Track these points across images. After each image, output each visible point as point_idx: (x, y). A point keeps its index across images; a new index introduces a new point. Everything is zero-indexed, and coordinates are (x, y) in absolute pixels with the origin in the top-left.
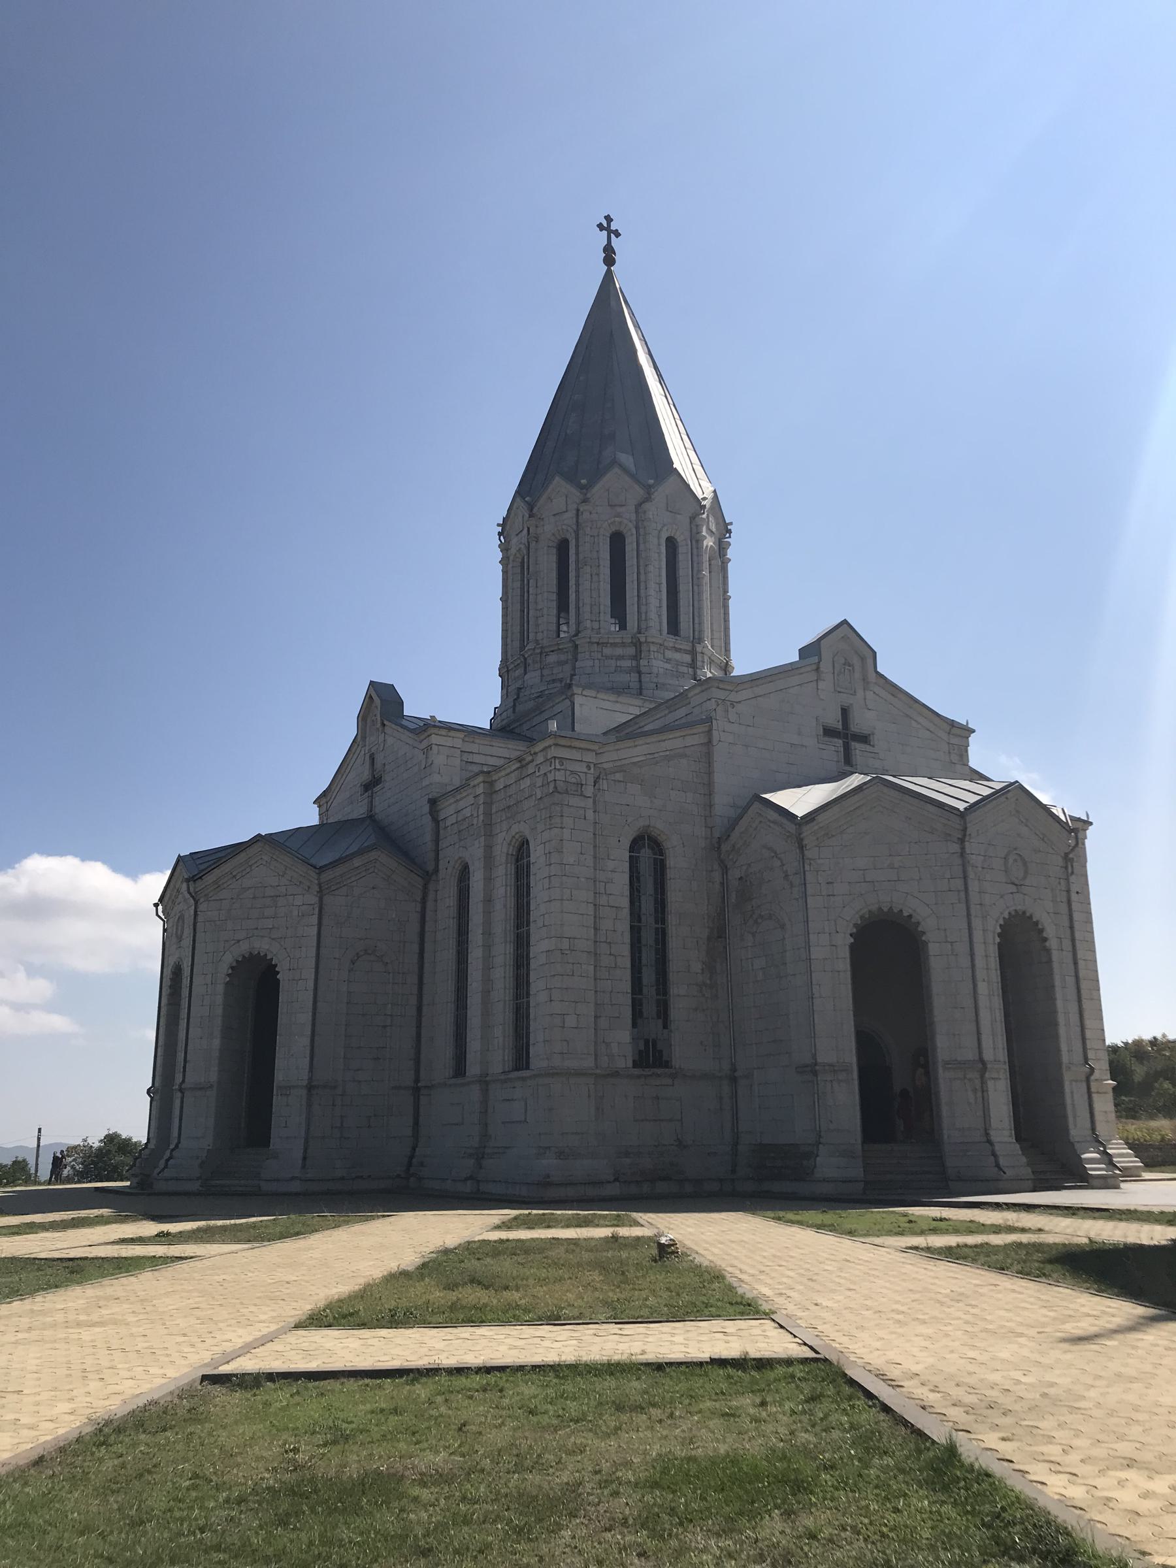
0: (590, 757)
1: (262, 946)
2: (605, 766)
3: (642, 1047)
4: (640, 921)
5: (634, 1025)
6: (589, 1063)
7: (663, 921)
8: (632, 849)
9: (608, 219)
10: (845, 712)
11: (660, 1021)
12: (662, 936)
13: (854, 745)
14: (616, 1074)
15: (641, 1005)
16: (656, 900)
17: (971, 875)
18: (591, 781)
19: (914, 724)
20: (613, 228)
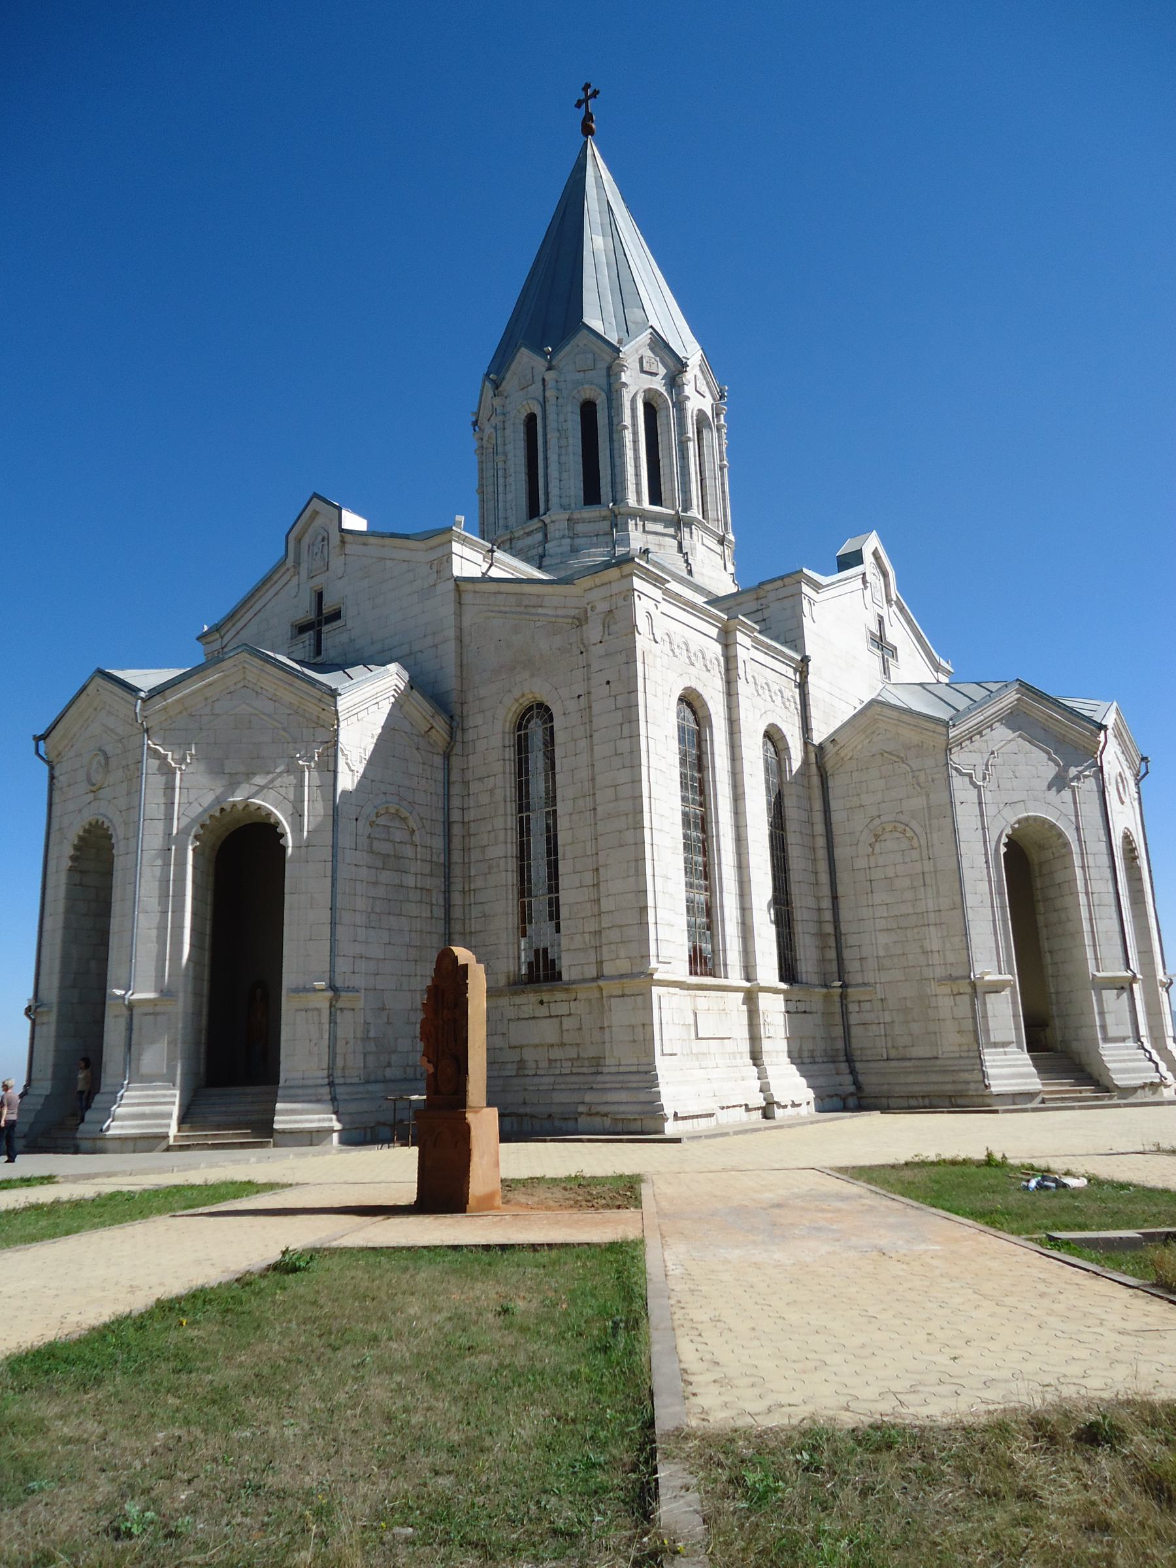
19: (389, 563)
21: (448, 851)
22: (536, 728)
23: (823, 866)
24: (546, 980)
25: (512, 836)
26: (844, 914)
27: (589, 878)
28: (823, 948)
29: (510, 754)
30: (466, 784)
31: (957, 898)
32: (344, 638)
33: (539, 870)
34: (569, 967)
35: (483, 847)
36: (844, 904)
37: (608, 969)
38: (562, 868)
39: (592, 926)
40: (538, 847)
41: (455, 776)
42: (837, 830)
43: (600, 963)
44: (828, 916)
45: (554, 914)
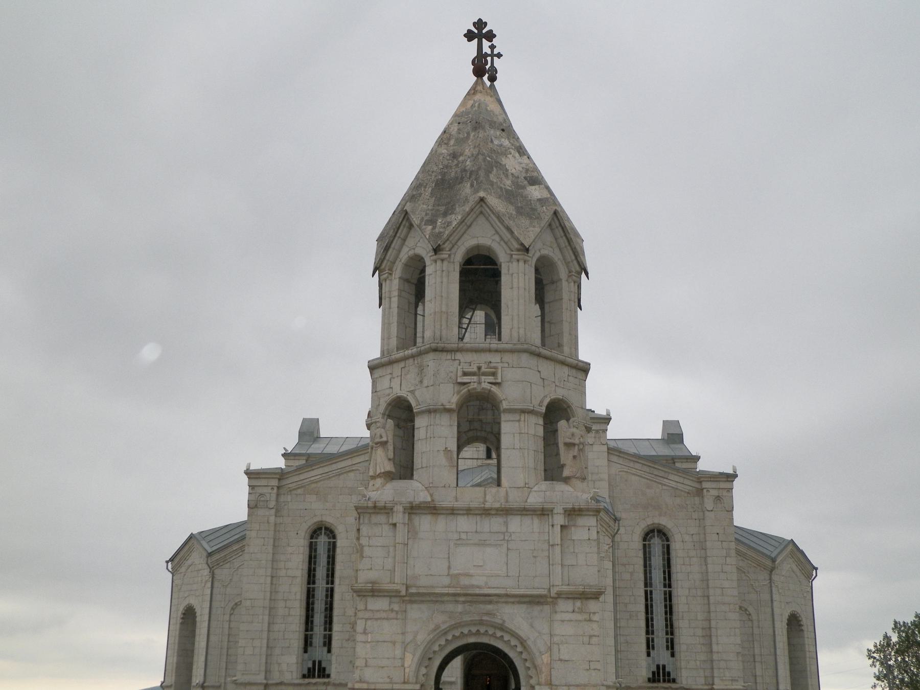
0: (275, 483)
1: (193, 601)
2: (290, 486)
3: (310, 665)
4: (314, 583)
5: (306, 651)
6: (260, 678)
7: (332, 583)
8: (312, 537)
11: (326, 649)
12: (330, 593)
14: (281, 684)
15: (311, 638)
16: (328, 570)
18: (274, 496)
20: (496, 52)
22: (656, 544)
24: (664, 681)
27: (699, 632)
29: (641, 554)
31: (772, 650)
35: (626, 605)
39: (703, 657)
45: (671, 646)
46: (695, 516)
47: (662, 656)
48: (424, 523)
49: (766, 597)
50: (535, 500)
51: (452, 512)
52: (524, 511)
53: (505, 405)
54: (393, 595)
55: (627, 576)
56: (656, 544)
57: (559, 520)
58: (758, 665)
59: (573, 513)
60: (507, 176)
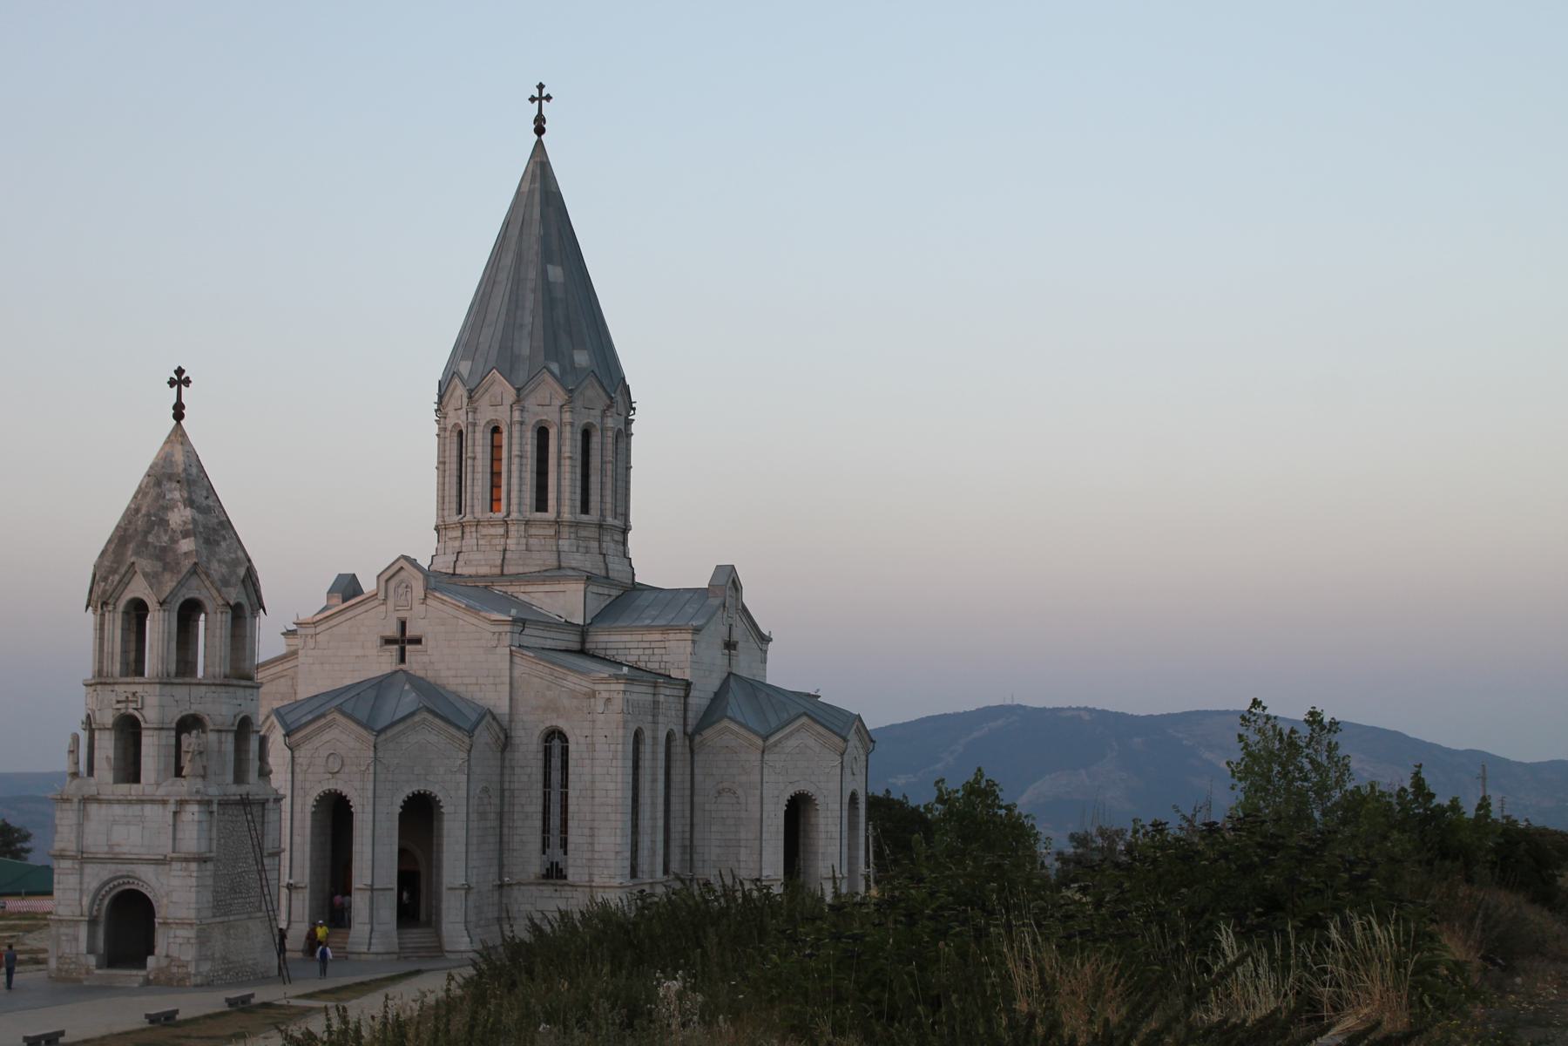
9: (541, 87)
10: (403, 624)
13: (408, 647)
17: (297, 769)
21: (502, 805)
22: (556, 743)
23: (688, 807)
25: (540, 801)
26: (697, 835)
27: (587, 832)
28: (683, 853)
29: (541, 756)
30: (513, 768)
32: (426, 659)
33: (555, 821)
34: (573, 875)
36: (696, 829)
37: (597, 881)
38: (570, 823)
39: (588, 855)
40: (555, 809)
41: (507, 763)
42: (697, 786)
43: (591, 875)
44: (687, 835)
45: (564, 844)
46: (589, 717)
47: (555, 853)
48: (93, 808)
49: (758, 778)
50: (160, 792)
51: (109, 802)
52: (153, 802)
53: (143, 725)
54: (73, 858)
55: (525, 778)
56: (556, 743)
57: (172, 808)
58: (743, 850)
59: (181, 803)
60: (166, 531)
